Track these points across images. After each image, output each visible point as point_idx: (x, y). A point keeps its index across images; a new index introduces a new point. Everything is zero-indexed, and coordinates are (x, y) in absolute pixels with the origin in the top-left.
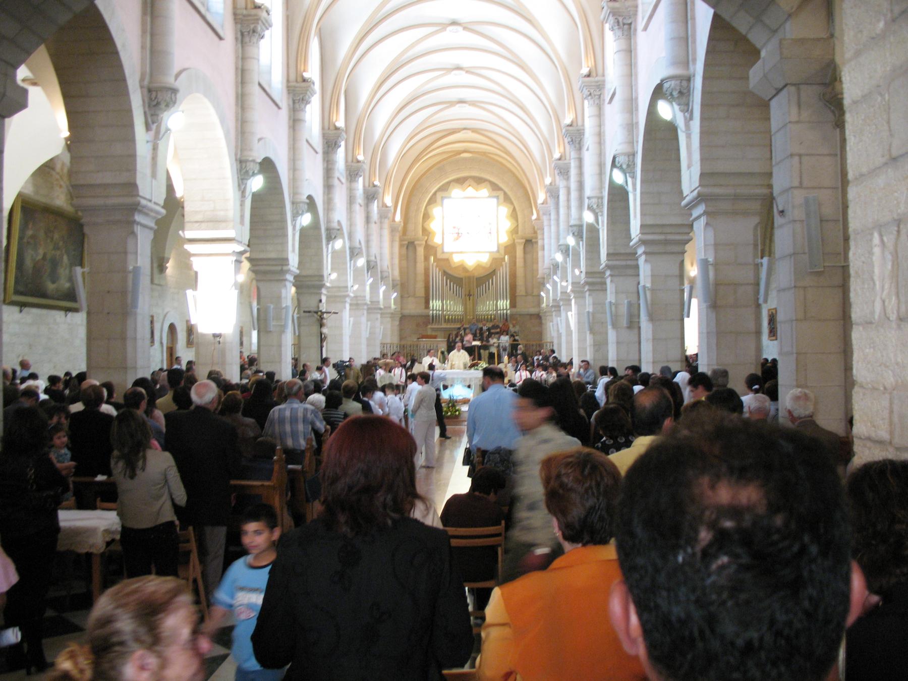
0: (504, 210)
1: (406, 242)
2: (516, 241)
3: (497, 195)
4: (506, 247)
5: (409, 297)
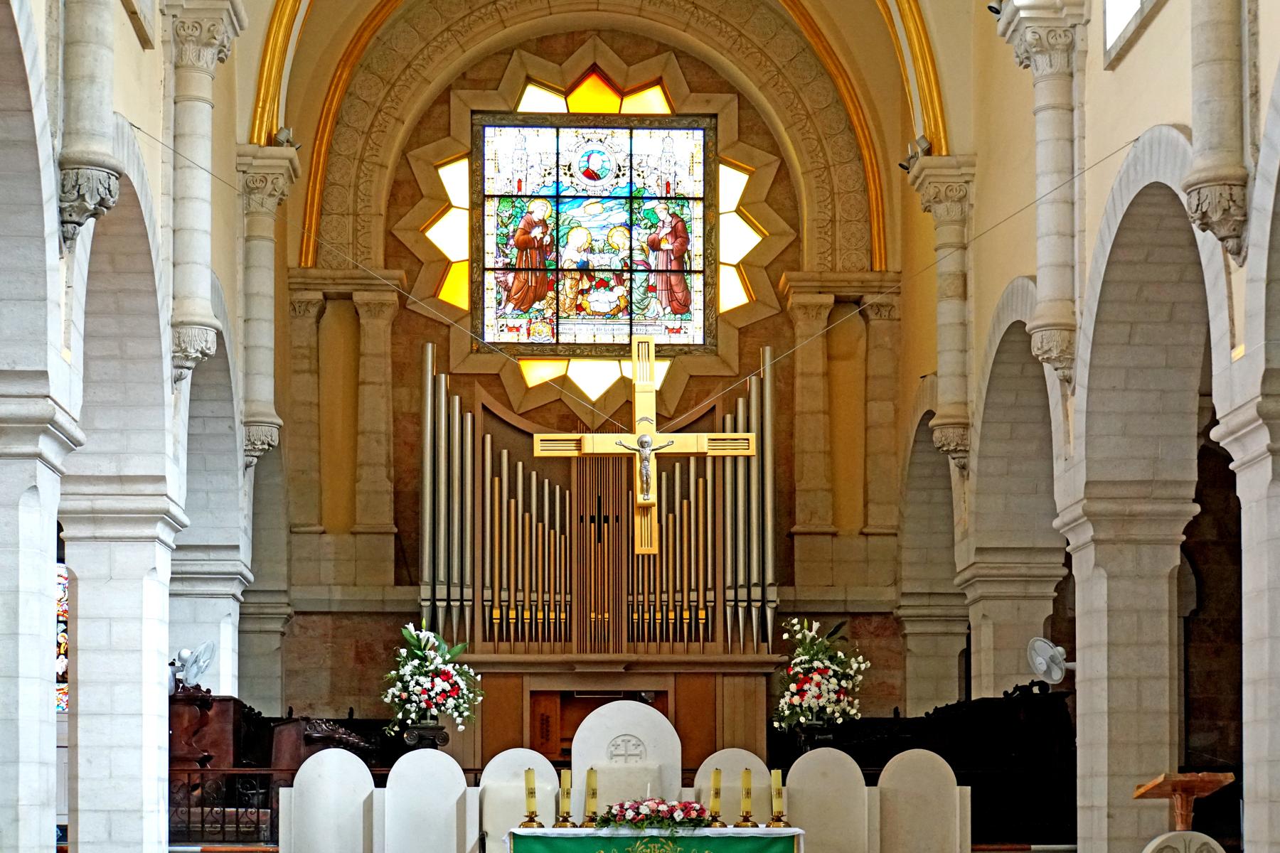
0: (732, 183)
1: (319, 296)
2: (793, 300)
3: (710, 110)
4: (743, 332)
5: (324, 532)
